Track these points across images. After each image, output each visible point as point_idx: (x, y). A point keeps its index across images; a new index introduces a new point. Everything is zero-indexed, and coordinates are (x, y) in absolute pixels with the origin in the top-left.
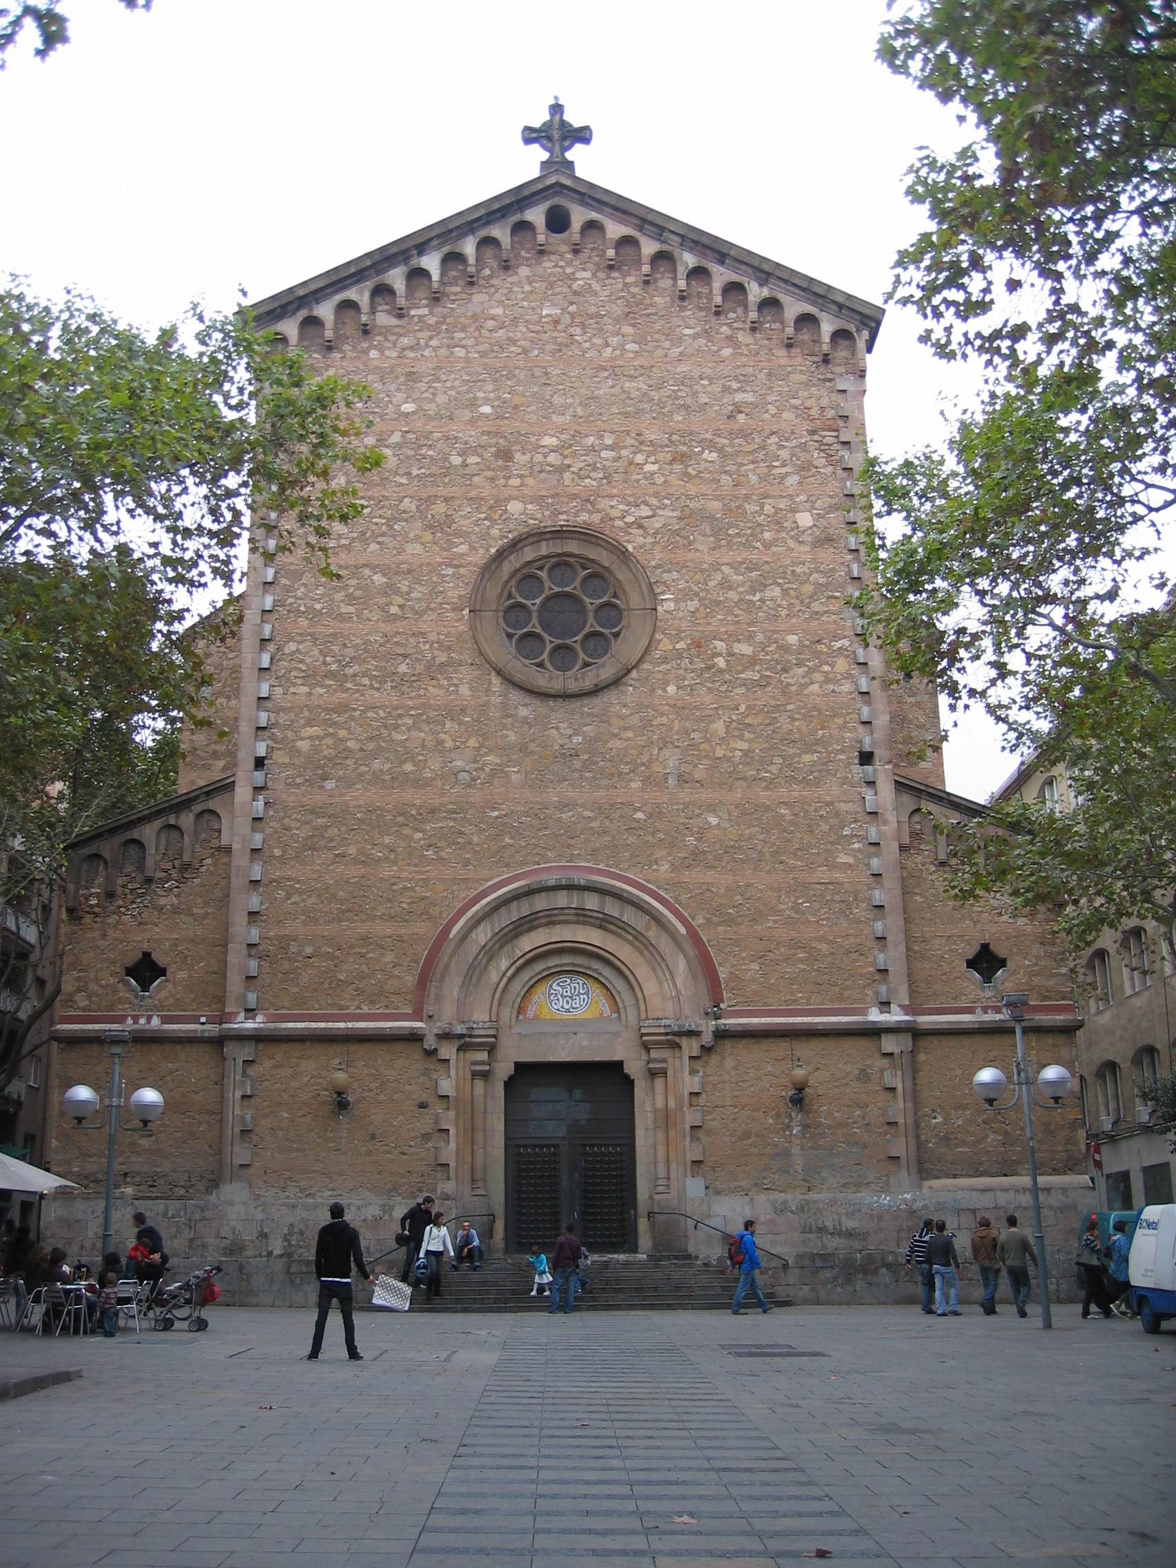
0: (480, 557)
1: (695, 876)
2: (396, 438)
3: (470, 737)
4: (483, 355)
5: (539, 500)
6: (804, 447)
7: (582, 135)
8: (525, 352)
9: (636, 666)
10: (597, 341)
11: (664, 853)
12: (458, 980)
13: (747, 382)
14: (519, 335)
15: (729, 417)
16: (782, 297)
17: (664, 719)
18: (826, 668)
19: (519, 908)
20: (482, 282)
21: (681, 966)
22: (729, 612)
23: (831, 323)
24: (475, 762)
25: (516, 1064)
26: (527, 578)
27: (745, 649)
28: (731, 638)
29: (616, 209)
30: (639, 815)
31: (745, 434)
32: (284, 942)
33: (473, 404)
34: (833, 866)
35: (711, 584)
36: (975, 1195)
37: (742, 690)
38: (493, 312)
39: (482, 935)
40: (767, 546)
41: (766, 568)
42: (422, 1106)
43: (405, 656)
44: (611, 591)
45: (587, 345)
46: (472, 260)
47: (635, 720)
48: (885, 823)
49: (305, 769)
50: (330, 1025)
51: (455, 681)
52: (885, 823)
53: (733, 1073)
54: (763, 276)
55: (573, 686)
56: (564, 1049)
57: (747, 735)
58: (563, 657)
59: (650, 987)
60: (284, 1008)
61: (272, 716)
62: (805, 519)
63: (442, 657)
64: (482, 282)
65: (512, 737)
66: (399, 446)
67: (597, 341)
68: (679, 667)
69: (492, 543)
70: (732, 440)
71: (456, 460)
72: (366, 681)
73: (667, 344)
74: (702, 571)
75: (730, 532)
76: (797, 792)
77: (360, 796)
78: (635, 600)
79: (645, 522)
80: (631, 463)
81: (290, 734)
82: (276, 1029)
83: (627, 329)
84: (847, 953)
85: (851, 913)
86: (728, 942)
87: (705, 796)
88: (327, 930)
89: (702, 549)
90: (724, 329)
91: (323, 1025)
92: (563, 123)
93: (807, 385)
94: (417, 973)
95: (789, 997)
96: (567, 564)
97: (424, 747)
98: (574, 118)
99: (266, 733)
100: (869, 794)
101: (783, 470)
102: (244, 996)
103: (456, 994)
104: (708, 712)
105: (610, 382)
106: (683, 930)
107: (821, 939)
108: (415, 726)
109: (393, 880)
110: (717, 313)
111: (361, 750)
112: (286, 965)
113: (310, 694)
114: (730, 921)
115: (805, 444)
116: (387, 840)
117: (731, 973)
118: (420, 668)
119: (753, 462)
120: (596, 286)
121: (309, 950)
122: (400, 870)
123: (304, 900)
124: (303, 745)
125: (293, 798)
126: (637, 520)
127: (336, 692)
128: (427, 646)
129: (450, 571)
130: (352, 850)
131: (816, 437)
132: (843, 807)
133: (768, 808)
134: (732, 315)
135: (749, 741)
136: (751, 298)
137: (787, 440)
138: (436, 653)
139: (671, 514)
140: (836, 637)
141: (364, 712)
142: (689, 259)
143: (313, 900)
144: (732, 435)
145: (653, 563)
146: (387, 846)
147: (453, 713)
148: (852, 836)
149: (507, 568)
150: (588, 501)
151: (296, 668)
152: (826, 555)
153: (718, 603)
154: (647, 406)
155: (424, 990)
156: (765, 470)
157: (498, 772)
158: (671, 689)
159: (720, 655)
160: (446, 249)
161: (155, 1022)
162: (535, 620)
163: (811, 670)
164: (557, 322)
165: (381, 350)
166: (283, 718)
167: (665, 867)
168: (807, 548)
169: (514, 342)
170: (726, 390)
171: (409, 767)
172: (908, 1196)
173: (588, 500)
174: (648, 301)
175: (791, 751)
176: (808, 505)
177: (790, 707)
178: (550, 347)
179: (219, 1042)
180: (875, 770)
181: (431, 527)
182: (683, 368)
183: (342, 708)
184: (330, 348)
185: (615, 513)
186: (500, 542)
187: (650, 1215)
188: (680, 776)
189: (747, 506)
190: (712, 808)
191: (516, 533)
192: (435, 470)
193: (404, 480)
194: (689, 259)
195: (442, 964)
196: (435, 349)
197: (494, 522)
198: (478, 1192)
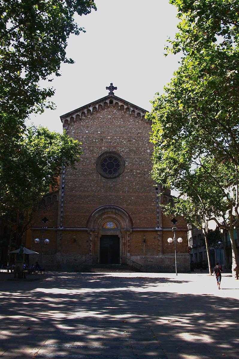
0: (97, 156)
1: (130, 207)
2: (85, 137)
4: (99, 123)
5: (107, 147)
7: (116, 88)
8: (106, 123)
10: (117, 122)
14: (105, 120)
17: (126, 182)
20: (99, 112)
21: (127, 221)
25: (102, 235)
28: (136, 170)
30: (121, 197)
31: (139, 137)
33: (97, 131)
34: (151, 206)
36: (171, 256)
37: (138, 178)
38: (101, 117)
39: (97, 215)
40: (143, 155)
42: (87, 241)
44: (118, 162)
46: (97, 108)
47: (121, 182)
48: (159, 199)
52: (159, 199)
58: (110, 172)
59: (122, 224)
63: (91, 172)
64: (99, 112)
65: (102, 185)
66: (85, 138)
67: (117, 122)
68: (128, 174)
71: (94, 140)
72: (79, 175)
73: (128, 122)
78: (122, 163)
80: (122, 141)
83: (122, 120)
87: (131, 194)
90: (137, 120)
96: (111, 157)
98: (114, 86)
99: (64, 183)
106: (128, 215)
110: (136, 118)
111: (79, 186)
113: (71, 177)
116: (82, 200)
119: (141, 142)
121: (70, 217)
124: (70, 185)
126: (122, 151)
129: (93, 158)
130: (77, 202)
134: (138, 118)
136: (141, 115)
141: (79, 180)
142: (132, 109)
144: (138, 137)
149: (102, 158)
150: (115, 147)
157: (100, 190)
158: (127, 177)
159: (135, 172)
160: (93, 106)
161: (47, 228)
162: (106, 166)
165: (83, 122)
167: (125, 205)
168: (149, 155)
169: (104, 122)
170: (137, 130)
171: (86, 189)
172: (161, 256)
174: (125, 115)
175: (145, 188)
178: (109, 122)
179: (56, 231)
181: (90, 151)
182: (130, 126)
183: (76, 180)
184: (75, 122)
185: (119, 149)
187: (122, 259)
190: (133, 196)
192: (91, 142)
193: (86, 144)
194: (132, 109)
196: (91, 122)
197: (100, 150)
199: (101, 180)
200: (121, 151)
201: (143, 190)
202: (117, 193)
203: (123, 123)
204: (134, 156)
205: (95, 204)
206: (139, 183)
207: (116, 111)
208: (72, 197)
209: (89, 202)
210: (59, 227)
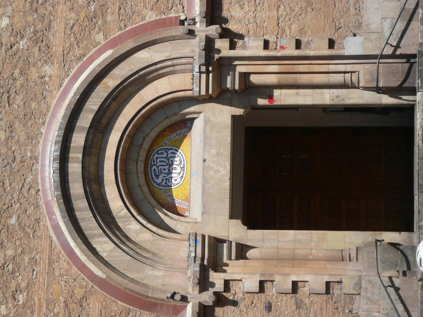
1: (57, 41)
11: (34, 70)
19: (81, 210)
39: (104, 245)
42: (269, 308)
53: (246, 8)
56: (218, 171)
86: (122, 11)
106: (109, 53)
117: (152, 9)
155: (156, 304)
167: (48, 69)
195: (131, 286)
198: (353, 255)
209: (21, 298)
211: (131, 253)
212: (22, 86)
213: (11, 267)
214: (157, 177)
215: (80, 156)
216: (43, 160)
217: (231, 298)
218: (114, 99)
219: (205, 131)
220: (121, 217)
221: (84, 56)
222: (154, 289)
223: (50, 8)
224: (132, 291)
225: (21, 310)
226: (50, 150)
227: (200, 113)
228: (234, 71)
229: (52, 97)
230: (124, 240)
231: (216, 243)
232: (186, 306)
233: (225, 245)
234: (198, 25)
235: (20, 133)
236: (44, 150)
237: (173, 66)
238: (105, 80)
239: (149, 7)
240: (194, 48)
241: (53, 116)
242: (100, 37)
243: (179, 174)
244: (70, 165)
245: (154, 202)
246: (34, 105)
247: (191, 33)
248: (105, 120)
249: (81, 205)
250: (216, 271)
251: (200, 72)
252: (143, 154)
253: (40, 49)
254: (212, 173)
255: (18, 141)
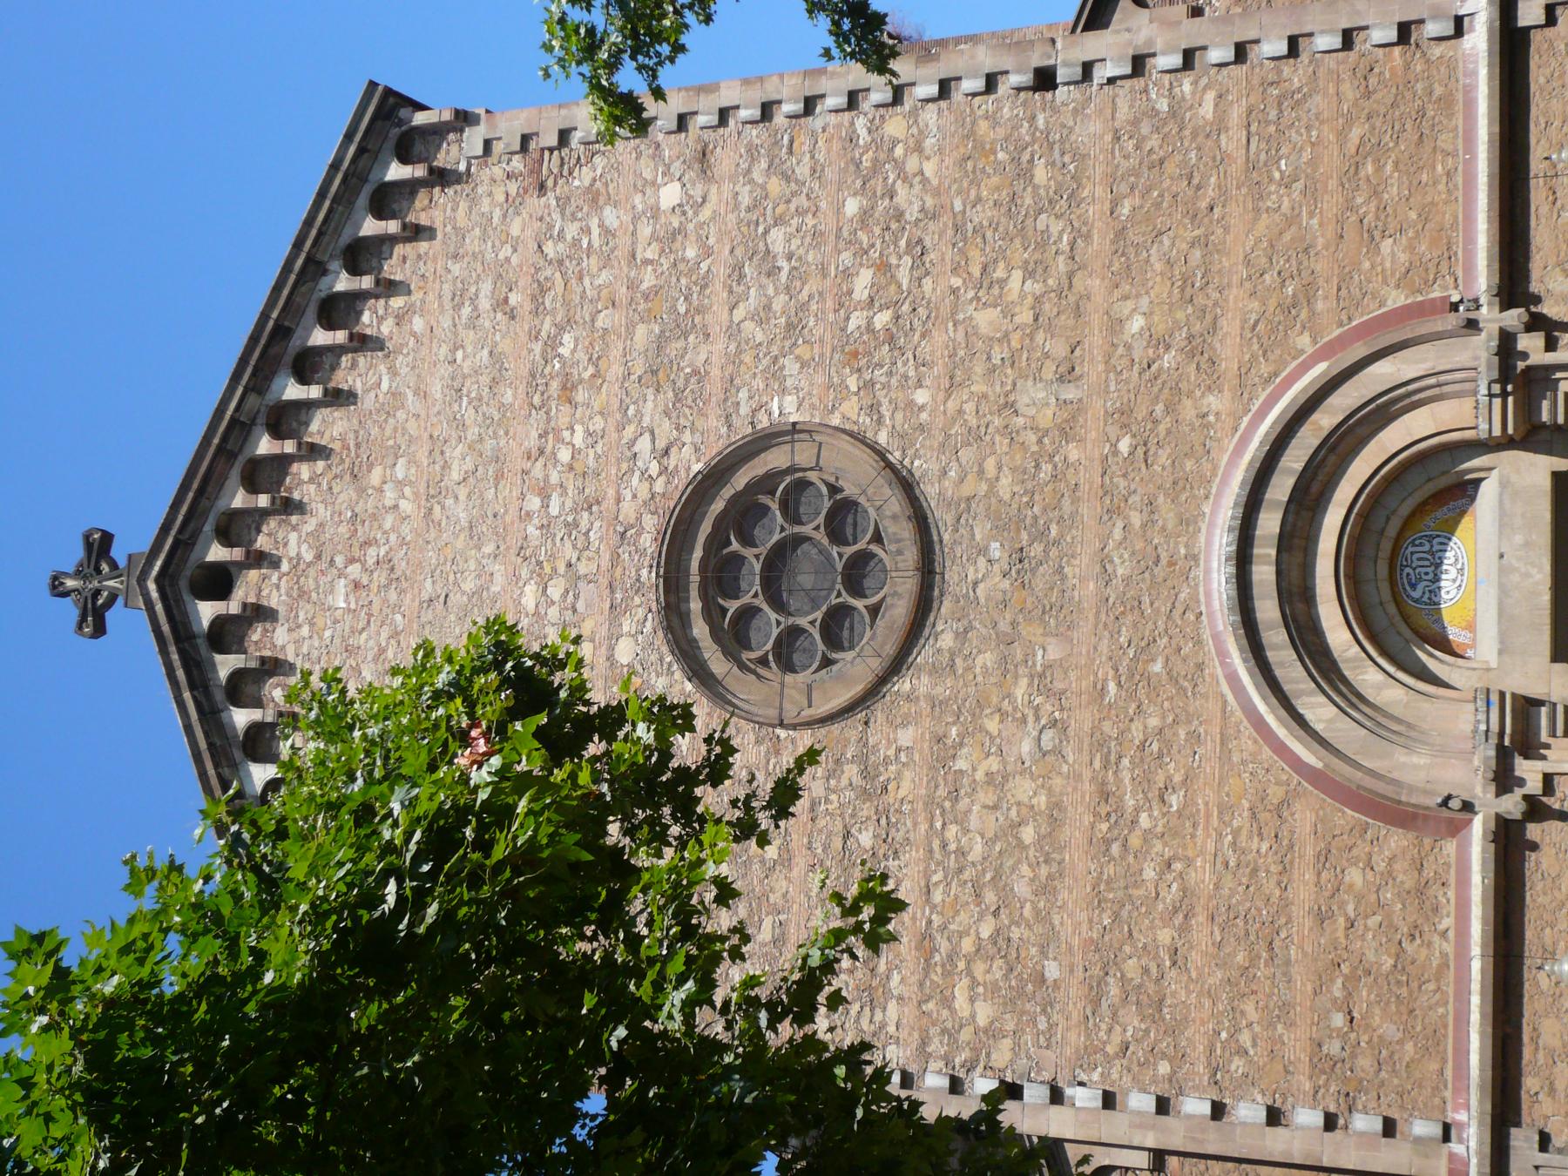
1: (1229, 350)
3: (982, 729)
6: (563, 203)
9: (881, 454)
10: (388, 522)
11: (1188, 403)
12: (1401, 757)
13: (464, 290)
14: (371, 643)
15: (513, 318)
16: (345, 239)
18: (899, 151)
19: (1276, 647)
22: (804, 307)
23: (386, 166)
24: (1024, 720)
26: (735, 636)
27: (863, 281)
28: (843, 301)
29: (201, 492)
30: (1124, 446)
32: (1323, 1065)
34: (1220, 125)
35: (760, 337)
37: (927, 283)
39: (1319, 710)
40: (708, 252)
41: (739, 252)
43: (847, 835)
45: (393, 537)
48: (1150, 42)
49: (1023, 1013)
50: (1476, 986)
51: (891, 752)
54: (312, 268)
55: (911, 555)
56: (1527, 575)
57: (1000, 273)
60: (1441, 1072)
61: (935, 1065)
62: (670, 195)
69: (678, 687)
70: (546, 312)
73: (401, 415)
74: (739, 352)
75: (682, 310)
76: (1095, 191)
77: (1074, 921)
79: (661, 444)
81: (966, 1035)
82: (1482, 1088)
83: (376, 476)
84: (1368, 94)
85: (1299, 90)
86: (1343, 292)
87: (1095, 340)
88: (1302, 983)
89: (709, 354)
91: (1475, 1000)
92: (78, 574)
93: (474, 201)
94: (1377, 827)
95: (1442, 187)
97: (995, 807)
100: (1101, 73)
101: (595, 231)
102: (1418, 1140)
103: (1422, 761)
104: (960, 336)
105: (449, 502)
107: (1342, 135)
108: (962, 821)
109: (1219, 865)
111: (996, 914)
112: (1365, 1063)
113: (900, 998)
114: (1309, 291)
115: (558, 199)
116: (1149, 873)
117: (1398, 286)
118: (867, 810)
119: (581, 278)
120: (310, 525)
121: (1339, 1020)
122: (1202, 853)
123: (1250, 1025)
125: (1072, 1036)
127: (898, 955)
128: (833, 797)
130: (1165, 936)
131: (550, 183)
132: (1124, 112)
133: (1120, 233)
135: (1010, 269)
137: (551, 227)
138: (844, 782)
139: (650, 404)
140: (852, 139)
143: (1249, 1007)
145: (724, 430)
146: (1161, 874)
147: (942, 752)
148: (1171, 96)
149: (718, 664)
151: (857, 1020)
152: (725, 160)
153: (790, 326)
154: (490, 444)
155: (1415, 816)
156: (594, 260)
157: (1042, 680)
158: (921, 397)
160: (238, 754)
163: (903, 176)
164: (357, 585)
166: (936, 1046)
167: (1213, 402)
168: (714, 189)
170: (472, 324)
171: (1028, 834)
173: (623, 534)
175: (1028, 201)
176: (648, 191)
177: (958, 206)
178: (393, 596)
180: (1066, 64)
182: (436, 390)
185: (644, 493)
186: (678, 675)
188: (1061, 379)
189: (645, 286)
190: (1116, 325)
191: (665, 649)
199: (934, 670)
200: (663, 470)
201: (1056, 227)
202: (1075, 501)
203: (401, 461)
204: (715, 330)
205: (1195, 737)
206: (976, 271)
207: (293, 536)
208: (1114, 990)
209: (1175, 801)
210: (1452, 1157)
211: (1368, 724)
212: (1169, 432)
213: (1155, 747)
214: (1413, 586)
215: (1273, 552)
216: (1208, 561)
217: (1557, 806)
218: (1332, 449)
219: (1501, 502)
220: (1346, 661)
221: (1276, 375)
222: (1412, 789)
223: (1215, 295)
224: (1370, 791)
225: (1174, 822)
226: (1219, 543)
227: (1491, 469)
228: (1555, 390)
229: (1222, 450)
230: (1354, 700)
231: (1527, 707)
232: (1471, 820)
233: (1544, 710)
234: (1484, 310)
235: (1167, 514)
236: (1209, 543)
237: (1439, 385)
238: (1315, 417)
239: (1392, 282)
240: (1479, 352)
241: (1225, 481)
242: (1304, 341)
243: (1454, 581)
244: (1255, 568)
245: (1408, 633)
246: (1189, 465)
247: (1472, 325)
248: (1315, 488)
249: (1276, 638)
250: (1526, 757)
251: (1491, 396)
252: (1386, 546)
253: (1198, 368)
254: (1515, 578)
255: (1164, 529)
